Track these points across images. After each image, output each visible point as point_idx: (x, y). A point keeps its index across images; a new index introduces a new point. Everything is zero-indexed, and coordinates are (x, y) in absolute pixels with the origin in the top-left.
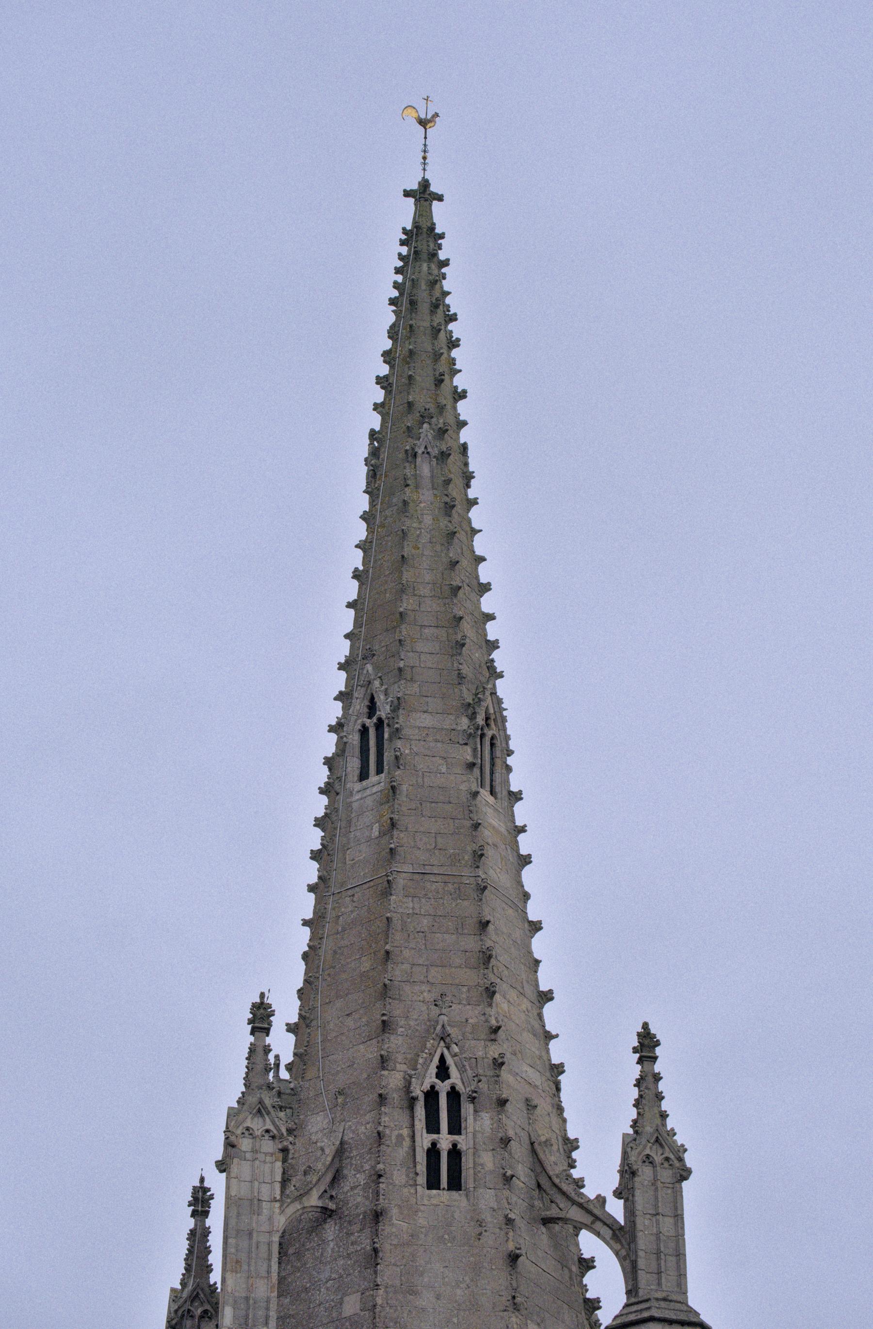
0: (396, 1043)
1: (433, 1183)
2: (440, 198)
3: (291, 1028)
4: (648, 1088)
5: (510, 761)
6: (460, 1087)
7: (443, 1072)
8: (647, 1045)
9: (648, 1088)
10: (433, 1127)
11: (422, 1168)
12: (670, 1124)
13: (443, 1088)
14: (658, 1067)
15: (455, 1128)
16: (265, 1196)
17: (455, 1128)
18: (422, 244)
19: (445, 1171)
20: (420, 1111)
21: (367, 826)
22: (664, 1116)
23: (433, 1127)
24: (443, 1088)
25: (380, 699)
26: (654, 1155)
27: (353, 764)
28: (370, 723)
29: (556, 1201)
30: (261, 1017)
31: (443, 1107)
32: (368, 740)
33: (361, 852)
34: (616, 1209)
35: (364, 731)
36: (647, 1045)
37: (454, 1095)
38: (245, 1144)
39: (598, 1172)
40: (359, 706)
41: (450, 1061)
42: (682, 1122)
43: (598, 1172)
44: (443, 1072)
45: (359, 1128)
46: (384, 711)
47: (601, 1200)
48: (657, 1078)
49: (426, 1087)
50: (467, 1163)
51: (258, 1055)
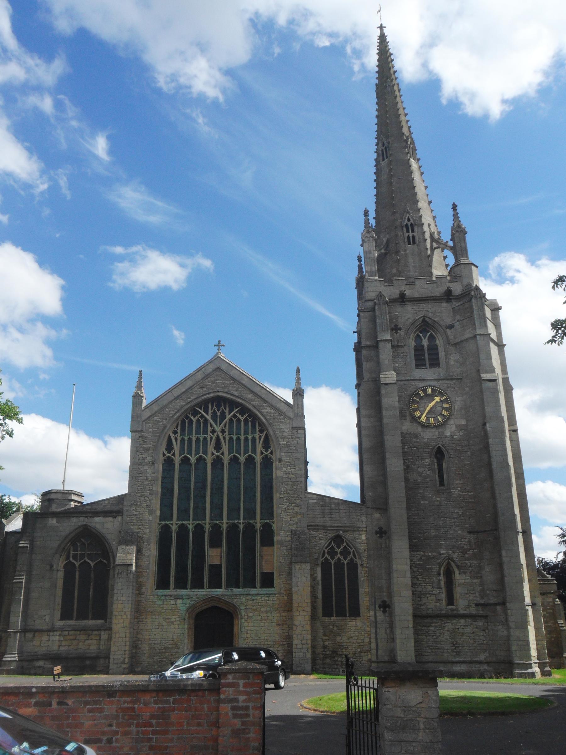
1: (409, 244)
2: (385, 27)
3: (374, 218)
4: (456, 216)
5: (416, 152)
6: (413, 223)
7: (409, 220)
8: (454, 207)
9: (456, 216)
10: (408, 232)
11: (406, 240)
12: (461, 223)
13: (409, 223)
14: (457, 211)
15: (413, 231)
16: (372, 250)
17: (413, 231)
20: (405, 229)
22: (460, 221)
23: (408, 232)
24: (409, 223)
25: (385, 142)
27: (381, 158)
28: (383, 148)
30: (366, 213)
33: (384, 177)
34: (451, 244)
35: (382, 150)
36: (454, 207)
37: (412, 225)
38: (366, 240)
40: (380, 145)
41: (410, 218)
42: (465, 223)
44: (409, 220)
46: (386, 144)
47: (447, 242)
48: (458, 213)
49: (405, 223)
50: (417, 238)
51: (367, 222)
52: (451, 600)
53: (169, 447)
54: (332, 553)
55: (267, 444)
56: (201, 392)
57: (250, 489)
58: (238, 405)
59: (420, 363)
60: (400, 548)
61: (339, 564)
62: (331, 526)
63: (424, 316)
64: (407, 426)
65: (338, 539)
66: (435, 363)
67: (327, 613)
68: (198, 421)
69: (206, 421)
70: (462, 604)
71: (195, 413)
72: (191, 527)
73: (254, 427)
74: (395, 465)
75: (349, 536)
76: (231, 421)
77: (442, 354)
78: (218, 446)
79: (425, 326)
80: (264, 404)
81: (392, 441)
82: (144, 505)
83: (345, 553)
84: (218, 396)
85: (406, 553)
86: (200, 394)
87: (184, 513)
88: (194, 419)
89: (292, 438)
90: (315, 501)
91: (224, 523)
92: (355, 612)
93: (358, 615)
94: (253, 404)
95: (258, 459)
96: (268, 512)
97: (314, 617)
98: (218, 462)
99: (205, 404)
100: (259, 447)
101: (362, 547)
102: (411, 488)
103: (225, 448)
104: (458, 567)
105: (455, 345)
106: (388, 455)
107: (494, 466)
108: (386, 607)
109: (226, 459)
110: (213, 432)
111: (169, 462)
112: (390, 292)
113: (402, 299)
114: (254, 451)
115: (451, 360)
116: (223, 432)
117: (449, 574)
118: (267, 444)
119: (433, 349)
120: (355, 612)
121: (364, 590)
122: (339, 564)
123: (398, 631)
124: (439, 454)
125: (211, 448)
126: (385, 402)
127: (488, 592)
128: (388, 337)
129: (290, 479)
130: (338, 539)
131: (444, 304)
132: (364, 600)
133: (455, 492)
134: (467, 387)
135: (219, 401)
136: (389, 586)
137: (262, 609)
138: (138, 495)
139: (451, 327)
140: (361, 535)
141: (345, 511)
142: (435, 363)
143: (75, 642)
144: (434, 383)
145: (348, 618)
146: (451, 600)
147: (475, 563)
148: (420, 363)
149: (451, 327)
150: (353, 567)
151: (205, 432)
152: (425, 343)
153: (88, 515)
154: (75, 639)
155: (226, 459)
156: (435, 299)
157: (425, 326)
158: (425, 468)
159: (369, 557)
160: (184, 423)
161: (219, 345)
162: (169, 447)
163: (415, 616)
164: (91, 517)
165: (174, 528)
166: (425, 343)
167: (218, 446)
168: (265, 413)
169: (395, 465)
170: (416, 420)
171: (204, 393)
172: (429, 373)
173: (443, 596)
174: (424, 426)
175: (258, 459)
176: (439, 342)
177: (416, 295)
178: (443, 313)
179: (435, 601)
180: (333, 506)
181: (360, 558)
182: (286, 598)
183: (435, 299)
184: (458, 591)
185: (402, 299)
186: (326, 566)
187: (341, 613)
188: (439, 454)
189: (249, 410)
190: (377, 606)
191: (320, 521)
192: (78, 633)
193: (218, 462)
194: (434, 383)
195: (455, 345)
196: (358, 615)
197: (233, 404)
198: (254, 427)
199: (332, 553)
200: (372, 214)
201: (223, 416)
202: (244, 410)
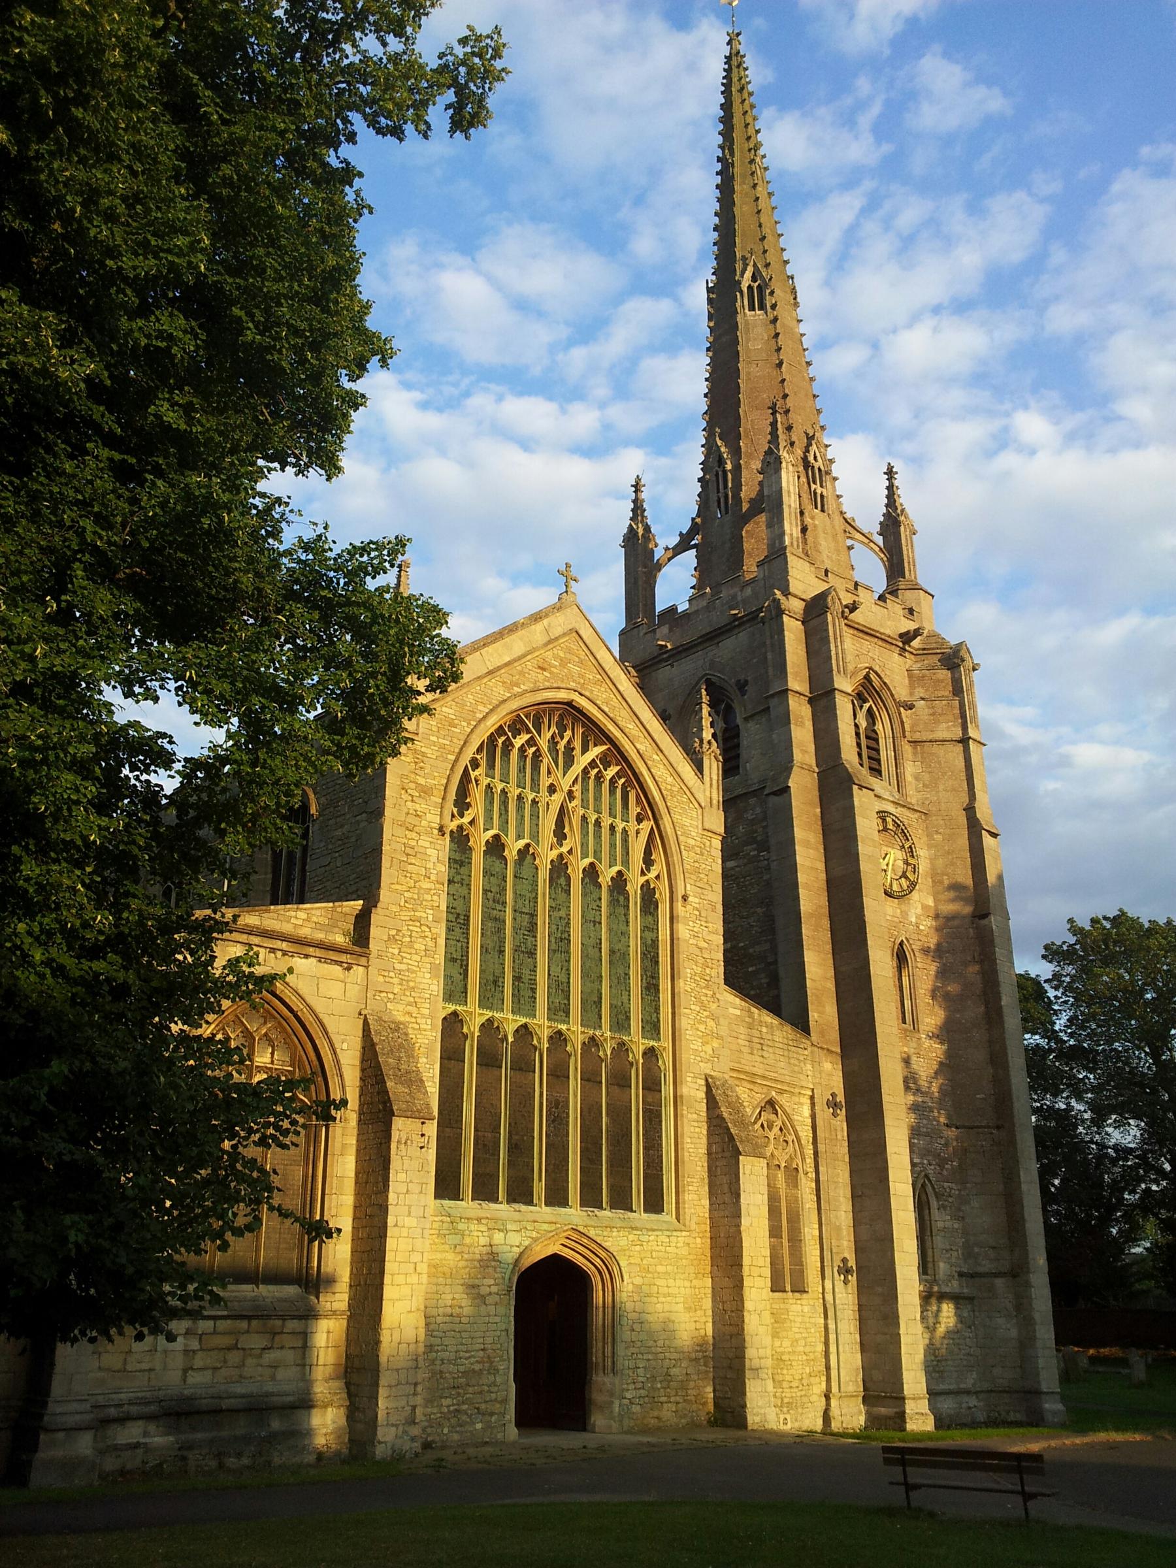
53: (462, 804)
56: (541, 678)
57: (619, 957)
62: (764, 1077)
63: (871, 668)
76: (585, 771)
77: (886, 754)
80: (655, 757)
82: (419, 946)
84: (570, 704)
89: (702, 854)
90: (738, 1012)
104: (936, 1193)
105: (914, 743)
127: (976, 1250)
129: (701, 949)
134: (937, 833)
137: (660, 1269)
138: (405, 915)
140: (802, 1104)
141: (781, 1046)
143: (234, 1357)
145: (790, 1294)
151: (535, 786)
153: (279, 944)
154: (235, 1347)
156: (886, 641)
164: (285, 953)
171: (547, 684)
176: (883, 728)
180: (764, 1030)
181: (803, 1159)
182: (699, 1240)
183: (886, 641)
189: (624, 758)
190: (836, 1269)
192: (244, 1325)
193: (559, 868)
195: (914, 743)
197: (594, 732)
202: (616, 754)
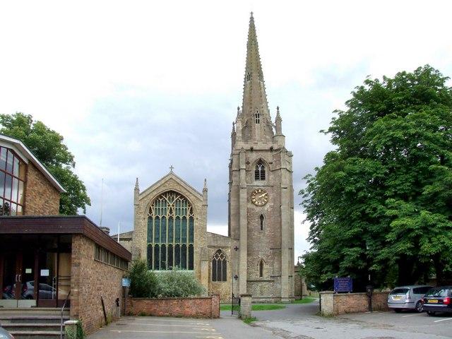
0: (252, 109)
4: (278, 112)
8: (278, 108)
9: (278, 112)
18: (252, 19)
19: (258, 122)
21: (248, 86)
26: (279, 119)
29: (268, 124)
30: (239, 108)
31: (258, 116)
32: (248, 77)
33: (248, 89)
39: (273, 120)
42: (281, 115)
43: (273, 120)
45: (248, 118)
51: (238, 112)
52: (261, 275)
53: (151, 212)
54: (217, 256)
55: (191, 212)
57: (184, 231)
58: (180, 194)
59: (257, 178)
60: (243, 254)
61: (219, 261)
64: (250, 205)
65: (219, 251)
66: (263, 178)
67: (214, 279)
68: (162, 201)
69: (166, 201)
70: (265, 277)
71: (161, 197)
72: (160, 246)
73: (186, 204)
74: (244, 222)
75: (224, 250)
77: (266, 174)
78: (171, 212)
79: (260, 162)
81: (243, 212)
83: (222, 256)
85: (246, 257)
86: (163, 189)
87: (157, 239)
88: (161, 200)
91: (174, 244)
92: (225, 279)
93: (226, 280)
94: (186, 194)
95: (188, 217)
96: (192, 240)
97: (209, 282)
98: (171, 218)
99: (165, 194)
100: (188, 213)
101: (228, 254)
102: (249, 230)
103: (174, 213)
106: (241, 218)
107: (283, 223)
108: (236, 277)
109: (174, 217)
110: (169, 206)
111: (150, 218)
112: (248, 146)
113: (252, 150)
114: (186, 214)
115: (270, 177)
116: (173, 206)
117: (261, 265)
118: (191, 212)
119: (263, 172)
120: (225, 279)
121: (228, 271)
122: (219, 261)
123: (240, 286)
124: (262, 217)
125: (168, 212)
126: (241, 195)
128: (244, 167)
130: (219, 251)
131: (269, 153)
132: (229, 275)
133: (267, 233)
135: (171, 192)
136: (238, 270)
139: (271, 163)
142: (263, 178)
144: (263, 188)
146: (261, 275)
147: (272, 261)
148: (257, 178)
149: (271, 163)
150: (225, 262)
152: (260, 169)
155: (174, 217)
156: (266, 151)
157: (260, 162)
158: (256, 223)
159: (231, 258)
160: (156, 201)
161: (172, 168)
162: (151, 212)
163: (247, 281)
165: (153, 246)
166: (260, 169)
167: (171, 212)
168: (191, 198)
169: (244, 222)
170: (253, 203)
172: (259, 183)
173: (259, 273)
174: (257, 206)
175: (188, 217)
176: (266, 169)
177: (258, 149)
178: (268, 157)
179: (256, 276)
183: (266, 151)
184: (264, 271)
185: (252, 150)
186: (214, 262)
187: (219, 280)
188: (262, 217)
191: (213, 244)
193: (171, 218)
194: (263, 188)
196: (226, 280)
197: (177, 194)
198: (186, 204)
199: (217, 256)
200: (241, 109)
201: (173, 199)
202: (182, 197)
